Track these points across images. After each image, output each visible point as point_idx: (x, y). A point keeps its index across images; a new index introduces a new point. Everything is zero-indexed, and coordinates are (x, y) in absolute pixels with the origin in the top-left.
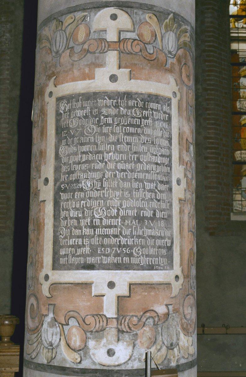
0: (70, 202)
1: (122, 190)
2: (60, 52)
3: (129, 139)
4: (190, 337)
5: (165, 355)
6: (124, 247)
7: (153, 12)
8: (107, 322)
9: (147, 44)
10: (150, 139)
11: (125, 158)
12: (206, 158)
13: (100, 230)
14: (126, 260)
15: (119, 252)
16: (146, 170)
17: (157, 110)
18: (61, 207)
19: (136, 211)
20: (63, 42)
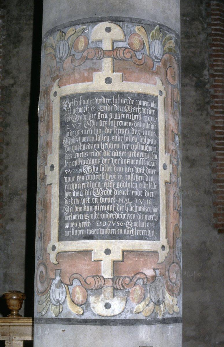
0: (72, 185)
1: (116, 174)
2: (64, 58)
3: (121, 131)
4: (175, 298)
5: (153, 309)
6: (118, 221)
7: (142, 25)
8: (104, 282)
9: (136, 51)
10: (140, 131)
11: (118, 146)
12: (214, 149)
13: (98, 207)
14: (120, 231)
15: (114, 225)
16: (137, 157)
17: (144, 107)
18: (66, 189)
19: (128, 191)
20: (66, 50)
